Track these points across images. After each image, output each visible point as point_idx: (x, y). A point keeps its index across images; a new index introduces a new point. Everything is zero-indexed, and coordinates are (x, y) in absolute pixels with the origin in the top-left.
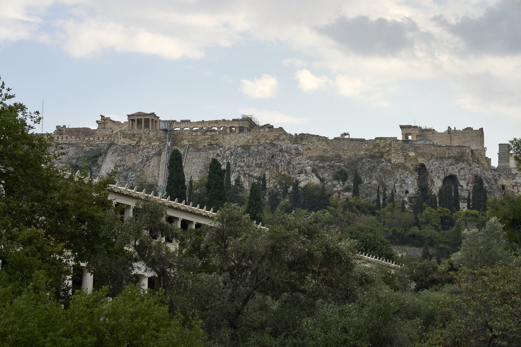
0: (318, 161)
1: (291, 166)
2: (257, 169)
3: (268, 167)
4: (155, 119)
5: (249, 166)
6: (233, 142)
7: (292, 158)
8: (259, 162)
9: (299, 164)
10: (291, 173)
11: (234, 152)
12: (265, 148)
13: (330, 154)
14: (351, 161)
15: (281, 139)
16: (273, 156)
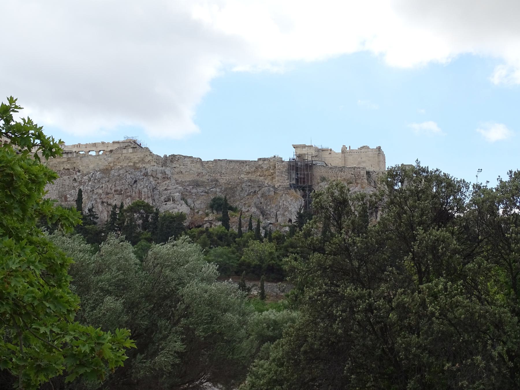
0: (191, 187)
1: (156, 192)
2: (116, 196)
3: (129, 194)
5: (107, 194)
6: (91, 166)
7: (158, 183)
8: (119, 188)
9: (166, 190)
11: (92, 176)
12: (127, 172)
13: (205, 178)
14: (230, 186)
15: (147, 161)
16: (136, 181)
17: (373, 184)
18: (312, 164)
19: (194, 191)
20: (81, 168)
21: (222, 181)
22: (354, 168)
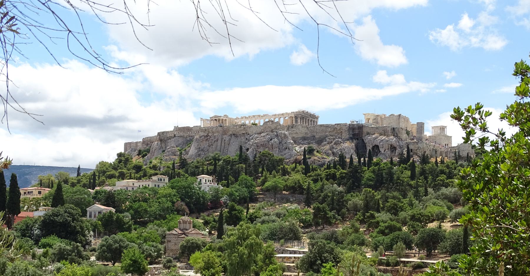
6: (254, 132)
13: (308, 136)
19: (302, 142)
21: (317, 137)
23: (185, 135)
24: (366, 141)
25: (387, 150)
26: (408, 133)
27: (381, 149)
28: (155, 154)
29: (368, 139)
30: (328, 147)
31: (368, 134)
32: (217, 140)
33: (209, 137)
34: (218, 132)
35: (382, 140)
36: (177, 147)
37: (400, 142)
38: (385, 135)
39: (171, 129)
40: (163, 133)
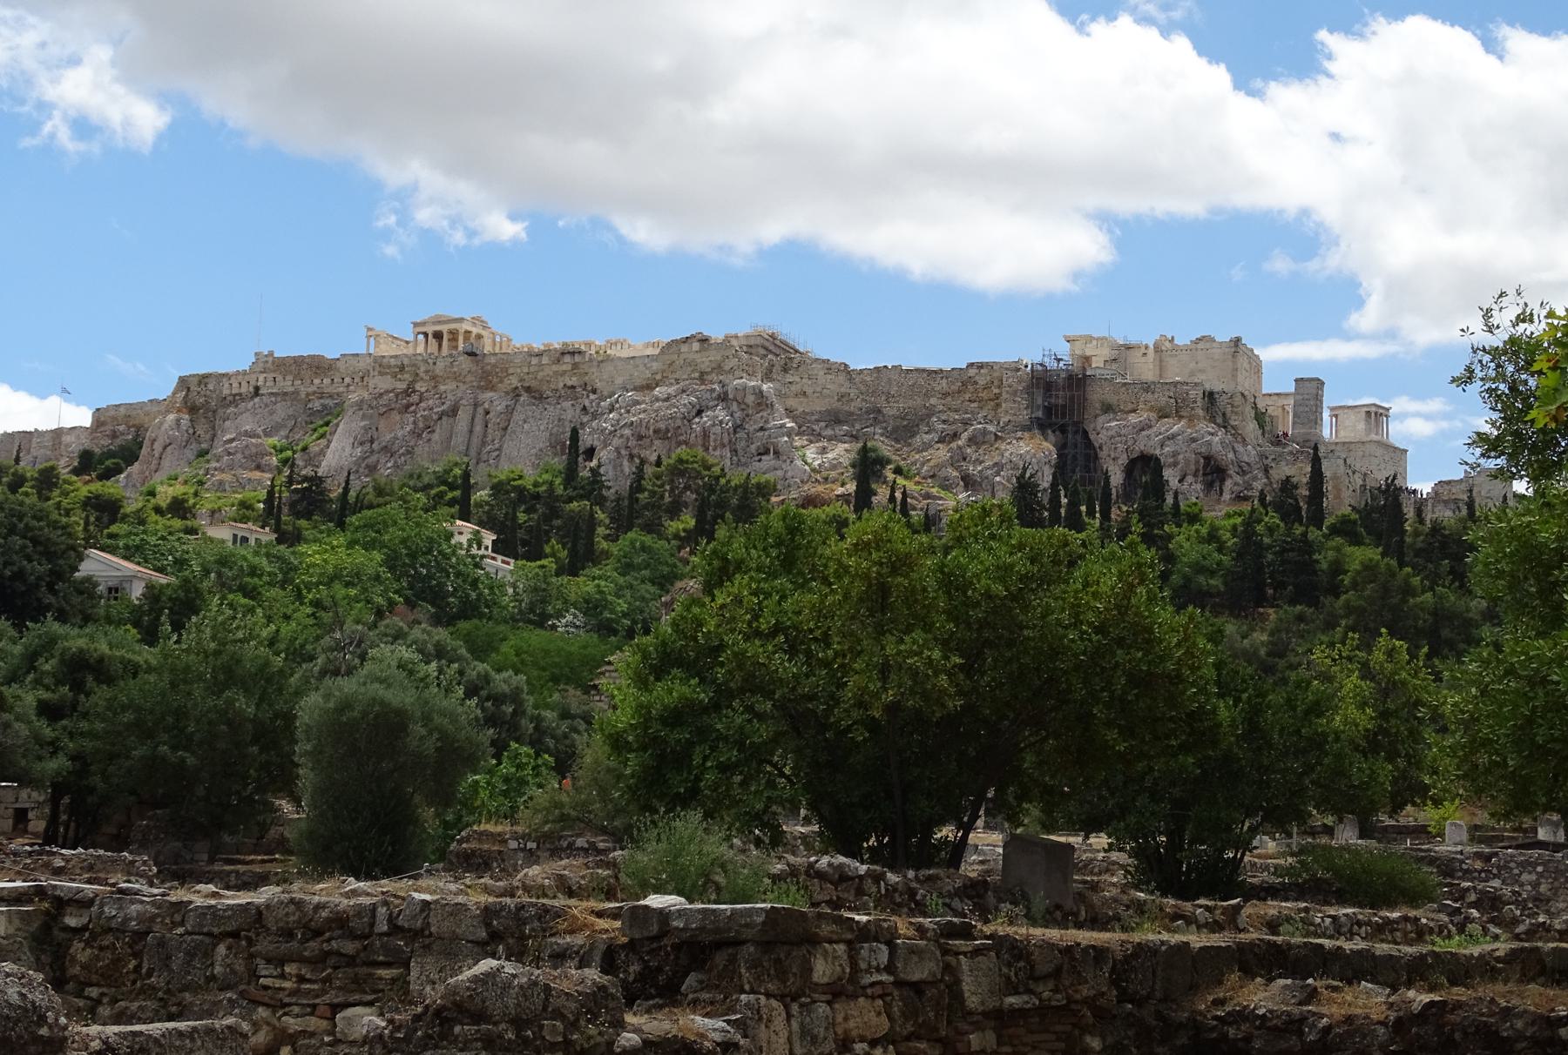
0: (823, 424)
2: (657, 442)
4: (475, 331)
5: (640, 438)
6: (619, 381)
9: (762, 429)
10: (740, 452)
13: (853, 407)
15: (727, 368)
17: (1220, 420)
18: (1085, 376)
19: (829, 432)
20: (598, 385)
21: (890, 411)
22: (1175, 384)
23: (303, 391)
24: (1098, 439)
25: (1190, 479)
26: (1260, 417)
27: (1168, 474)
28: (166, 463)
29: (1105, 430)
30: (942, 453)
31: (1108, 408)
32: (453, 412)
33: (415, 398)
34: (456, 377)
35: (1173, 437)
36: (267, 434)
37: (1239, 447)
38: (1181, 417)
39: (244, 363)
40: (203, 379)
